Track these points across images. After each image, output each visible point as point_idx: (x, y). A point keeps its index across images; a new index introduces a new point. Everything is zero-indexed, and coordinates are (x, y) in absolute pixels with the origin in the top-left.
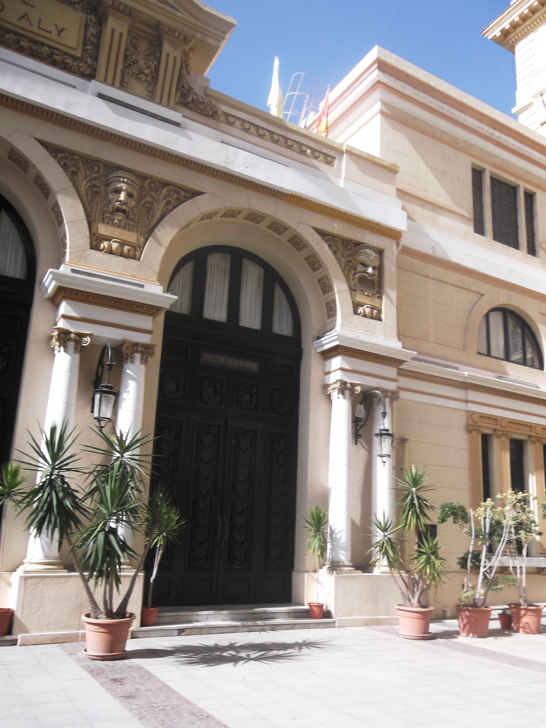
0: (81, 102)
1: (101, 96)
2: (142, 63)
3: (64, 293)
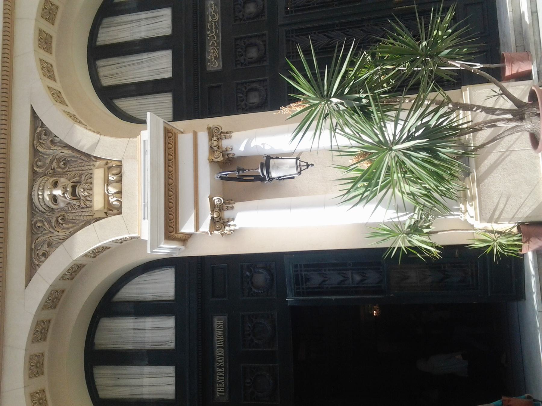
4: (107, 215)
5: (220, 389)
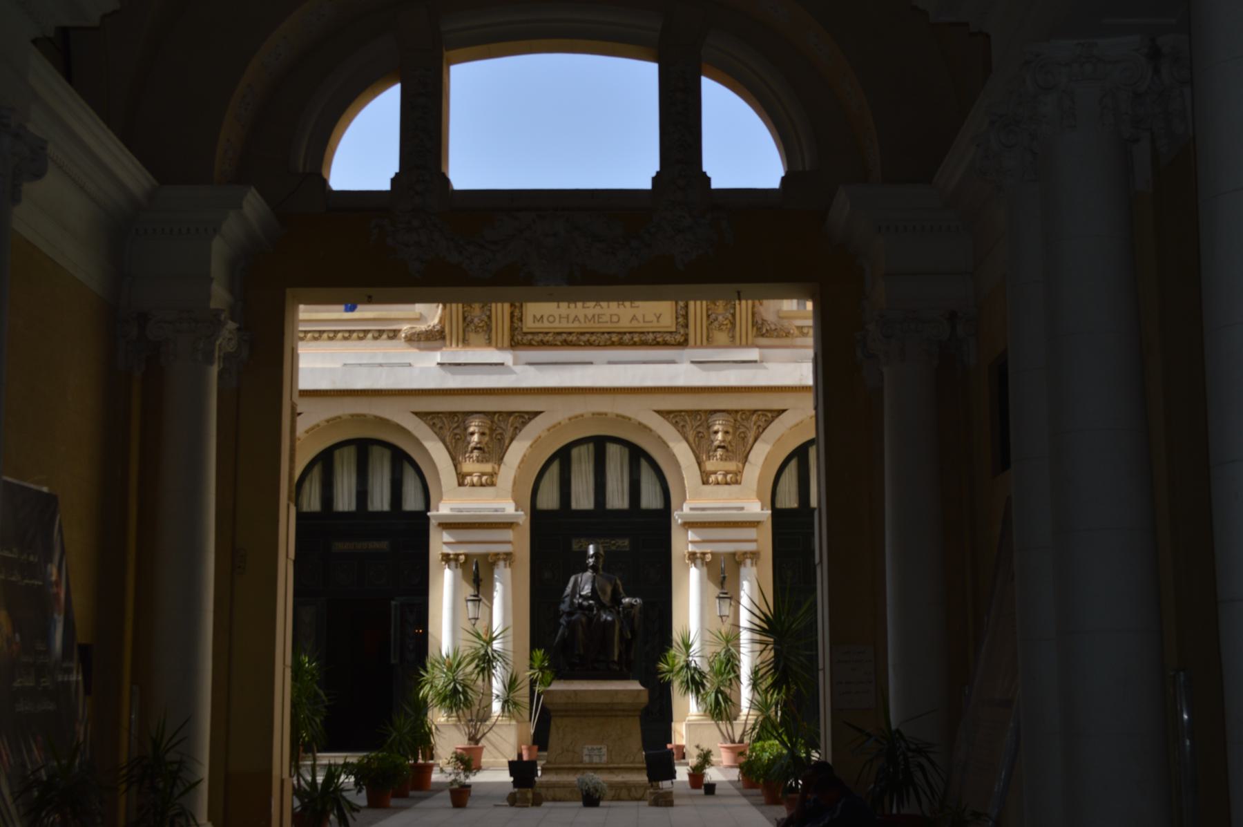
0: (679, 371)
1: (693, 362)
2: (720, 318)
3: (689, 525)
4: (458, 474)
5: (340, 546)
